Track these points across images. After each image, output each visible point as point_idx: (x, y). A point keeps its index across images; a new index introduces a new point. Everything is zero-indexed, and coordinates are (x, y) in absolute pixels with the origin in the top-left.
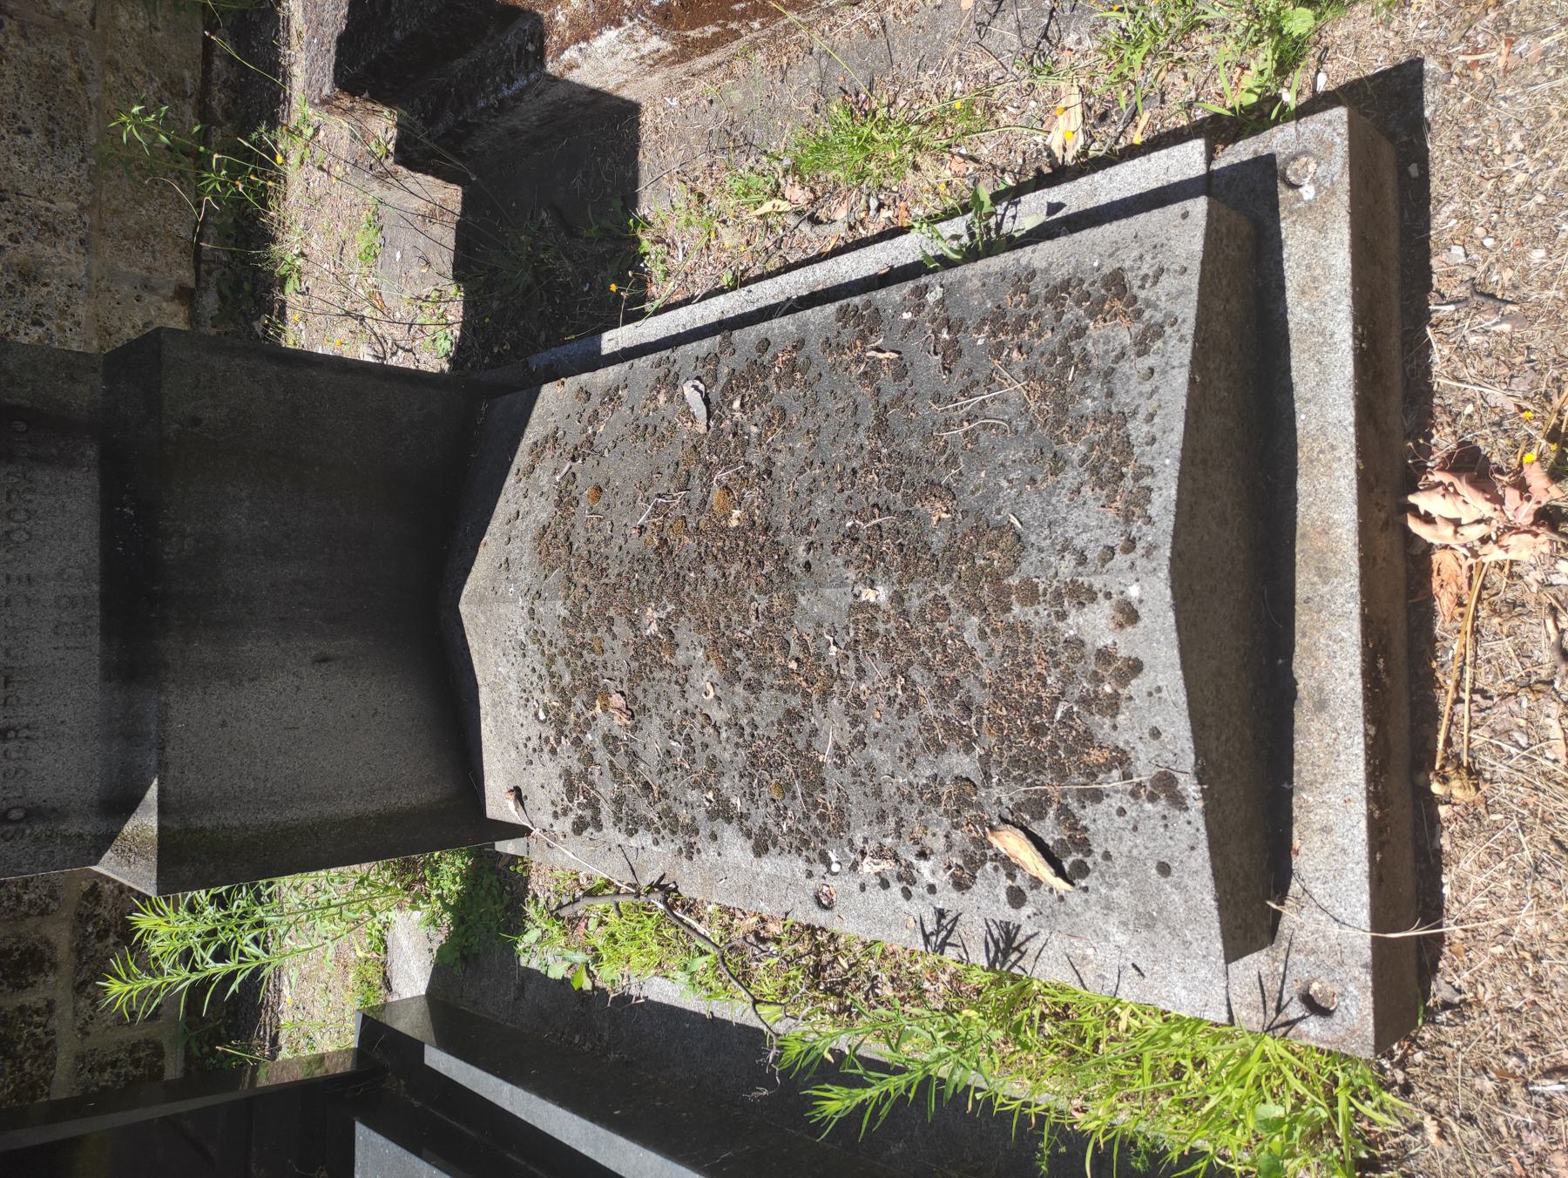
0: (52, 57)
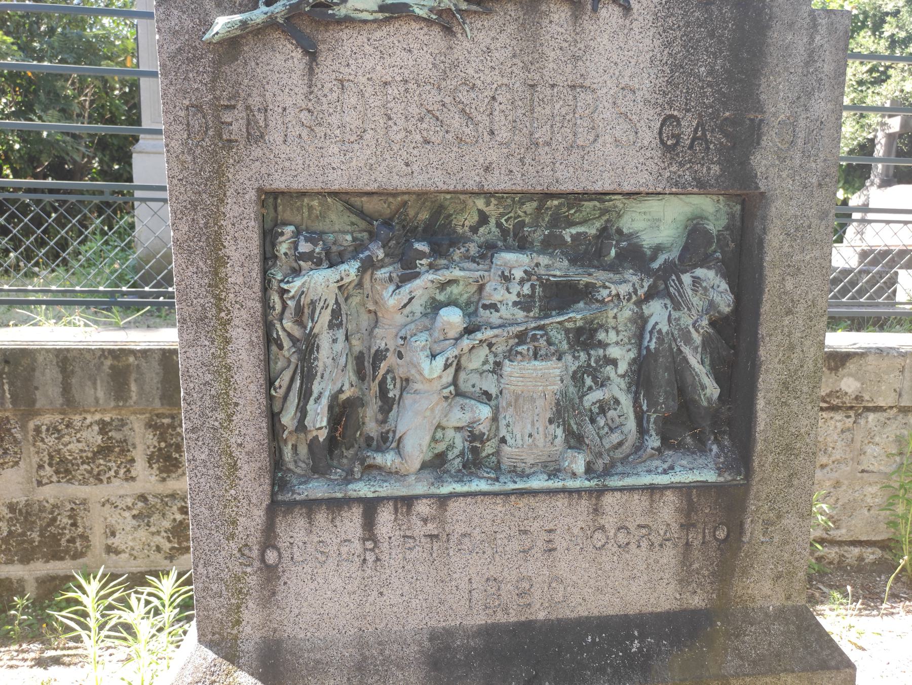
0: (833, 448)
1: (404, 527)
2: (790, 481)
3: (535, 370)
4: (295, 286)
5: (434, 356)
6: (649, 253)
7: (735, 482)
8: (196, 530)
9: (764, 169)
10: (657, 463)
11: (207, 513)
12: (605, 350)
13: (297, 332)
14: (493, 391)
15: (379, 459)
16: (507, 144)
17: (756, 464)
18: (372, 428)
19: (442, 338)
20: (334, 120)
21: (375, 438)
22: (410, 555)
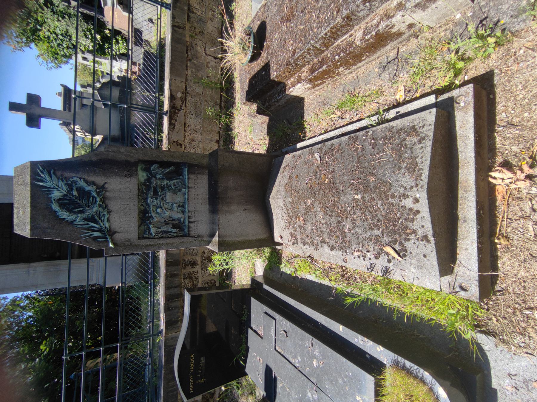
5: (165, 213)
13: (161, 234)
15: (182, 221)
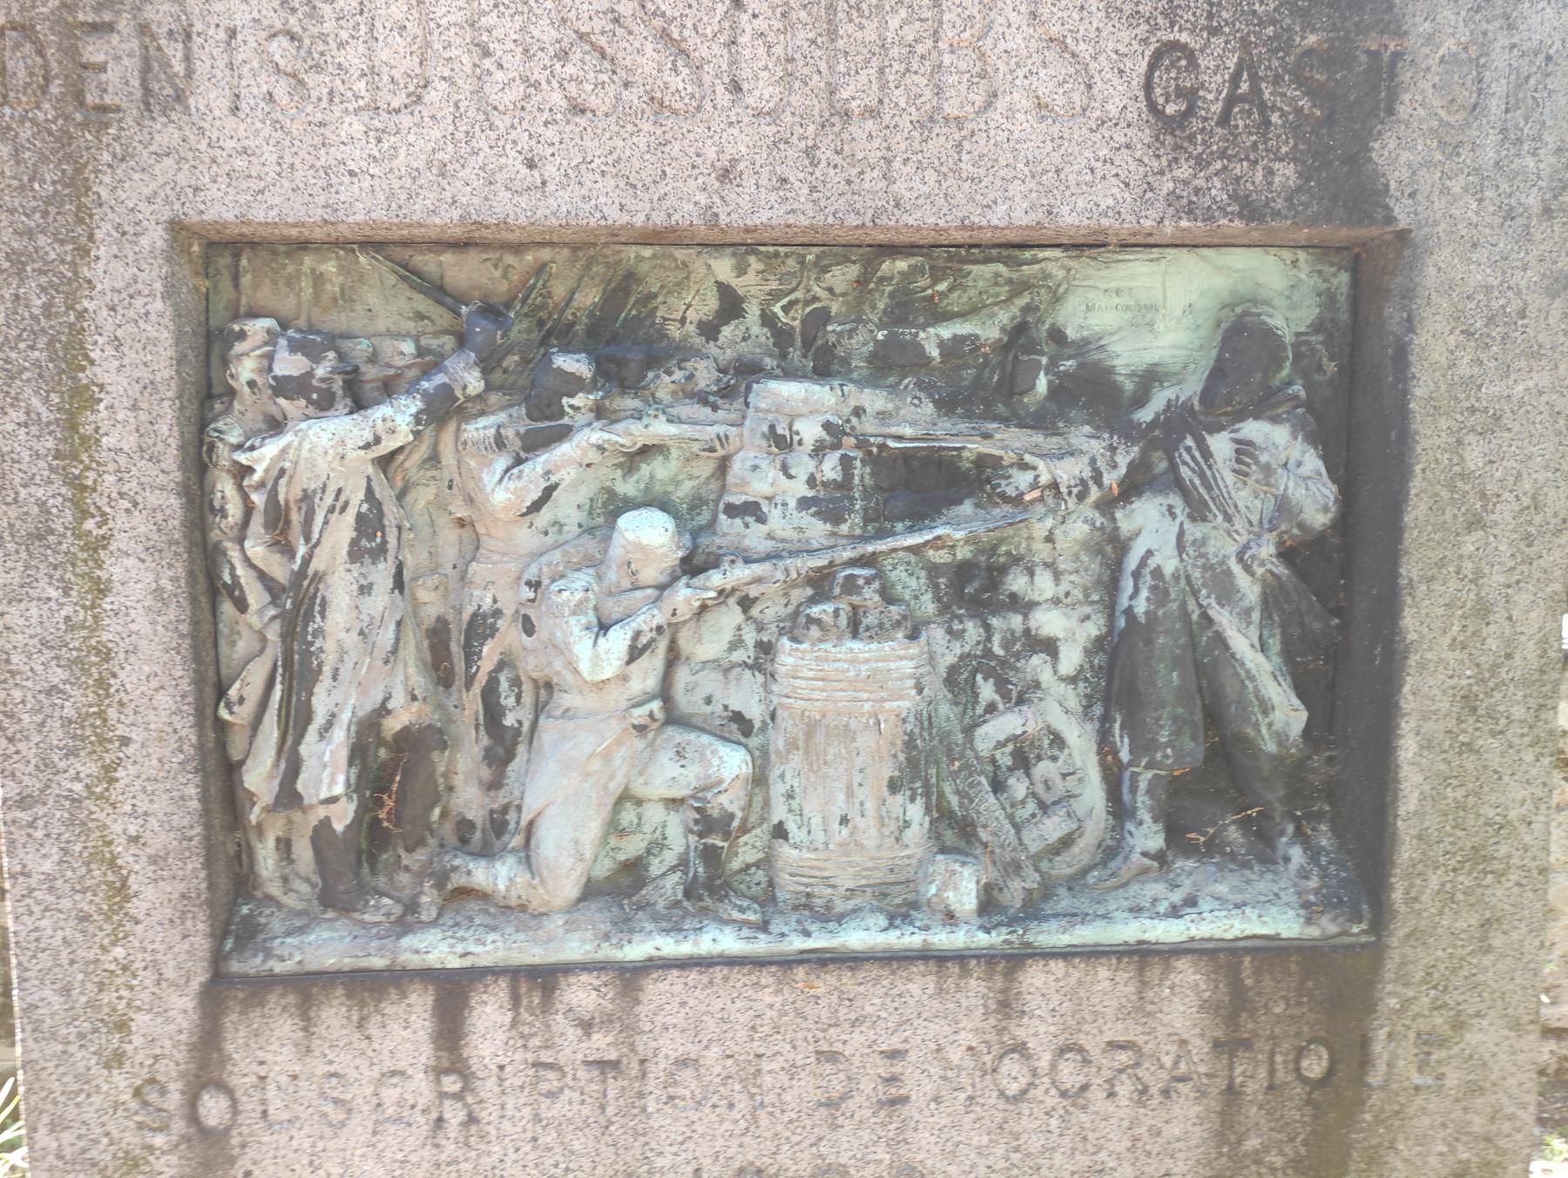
1: (536, 1042)
2: (1484, 938)
3: (853, 661)
4: (264, 456)
5: (604, 627)
6: (1129, 386)
7: (1347, 940)
8: (31, 1044)
9: (1405, 174)
10: (1156, 889)
11: (56, 1001)
12: (1026, 617)
13: (280, 570)
14: (755, 712)
16: (773, 115)
17: (1397, 896)
18: (470, 800)
19: (626, 584)
20: (353, 57)
21: (479, 824)
22: (550, 1111)
